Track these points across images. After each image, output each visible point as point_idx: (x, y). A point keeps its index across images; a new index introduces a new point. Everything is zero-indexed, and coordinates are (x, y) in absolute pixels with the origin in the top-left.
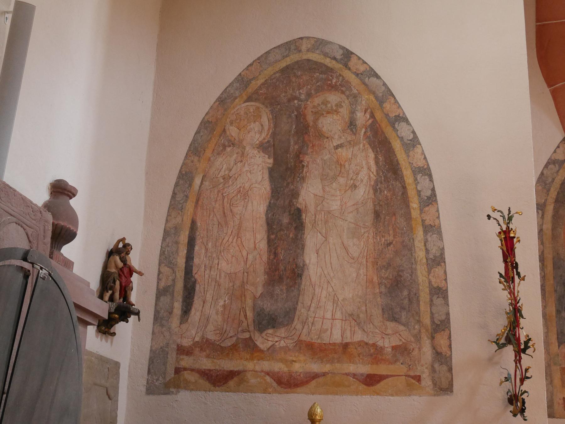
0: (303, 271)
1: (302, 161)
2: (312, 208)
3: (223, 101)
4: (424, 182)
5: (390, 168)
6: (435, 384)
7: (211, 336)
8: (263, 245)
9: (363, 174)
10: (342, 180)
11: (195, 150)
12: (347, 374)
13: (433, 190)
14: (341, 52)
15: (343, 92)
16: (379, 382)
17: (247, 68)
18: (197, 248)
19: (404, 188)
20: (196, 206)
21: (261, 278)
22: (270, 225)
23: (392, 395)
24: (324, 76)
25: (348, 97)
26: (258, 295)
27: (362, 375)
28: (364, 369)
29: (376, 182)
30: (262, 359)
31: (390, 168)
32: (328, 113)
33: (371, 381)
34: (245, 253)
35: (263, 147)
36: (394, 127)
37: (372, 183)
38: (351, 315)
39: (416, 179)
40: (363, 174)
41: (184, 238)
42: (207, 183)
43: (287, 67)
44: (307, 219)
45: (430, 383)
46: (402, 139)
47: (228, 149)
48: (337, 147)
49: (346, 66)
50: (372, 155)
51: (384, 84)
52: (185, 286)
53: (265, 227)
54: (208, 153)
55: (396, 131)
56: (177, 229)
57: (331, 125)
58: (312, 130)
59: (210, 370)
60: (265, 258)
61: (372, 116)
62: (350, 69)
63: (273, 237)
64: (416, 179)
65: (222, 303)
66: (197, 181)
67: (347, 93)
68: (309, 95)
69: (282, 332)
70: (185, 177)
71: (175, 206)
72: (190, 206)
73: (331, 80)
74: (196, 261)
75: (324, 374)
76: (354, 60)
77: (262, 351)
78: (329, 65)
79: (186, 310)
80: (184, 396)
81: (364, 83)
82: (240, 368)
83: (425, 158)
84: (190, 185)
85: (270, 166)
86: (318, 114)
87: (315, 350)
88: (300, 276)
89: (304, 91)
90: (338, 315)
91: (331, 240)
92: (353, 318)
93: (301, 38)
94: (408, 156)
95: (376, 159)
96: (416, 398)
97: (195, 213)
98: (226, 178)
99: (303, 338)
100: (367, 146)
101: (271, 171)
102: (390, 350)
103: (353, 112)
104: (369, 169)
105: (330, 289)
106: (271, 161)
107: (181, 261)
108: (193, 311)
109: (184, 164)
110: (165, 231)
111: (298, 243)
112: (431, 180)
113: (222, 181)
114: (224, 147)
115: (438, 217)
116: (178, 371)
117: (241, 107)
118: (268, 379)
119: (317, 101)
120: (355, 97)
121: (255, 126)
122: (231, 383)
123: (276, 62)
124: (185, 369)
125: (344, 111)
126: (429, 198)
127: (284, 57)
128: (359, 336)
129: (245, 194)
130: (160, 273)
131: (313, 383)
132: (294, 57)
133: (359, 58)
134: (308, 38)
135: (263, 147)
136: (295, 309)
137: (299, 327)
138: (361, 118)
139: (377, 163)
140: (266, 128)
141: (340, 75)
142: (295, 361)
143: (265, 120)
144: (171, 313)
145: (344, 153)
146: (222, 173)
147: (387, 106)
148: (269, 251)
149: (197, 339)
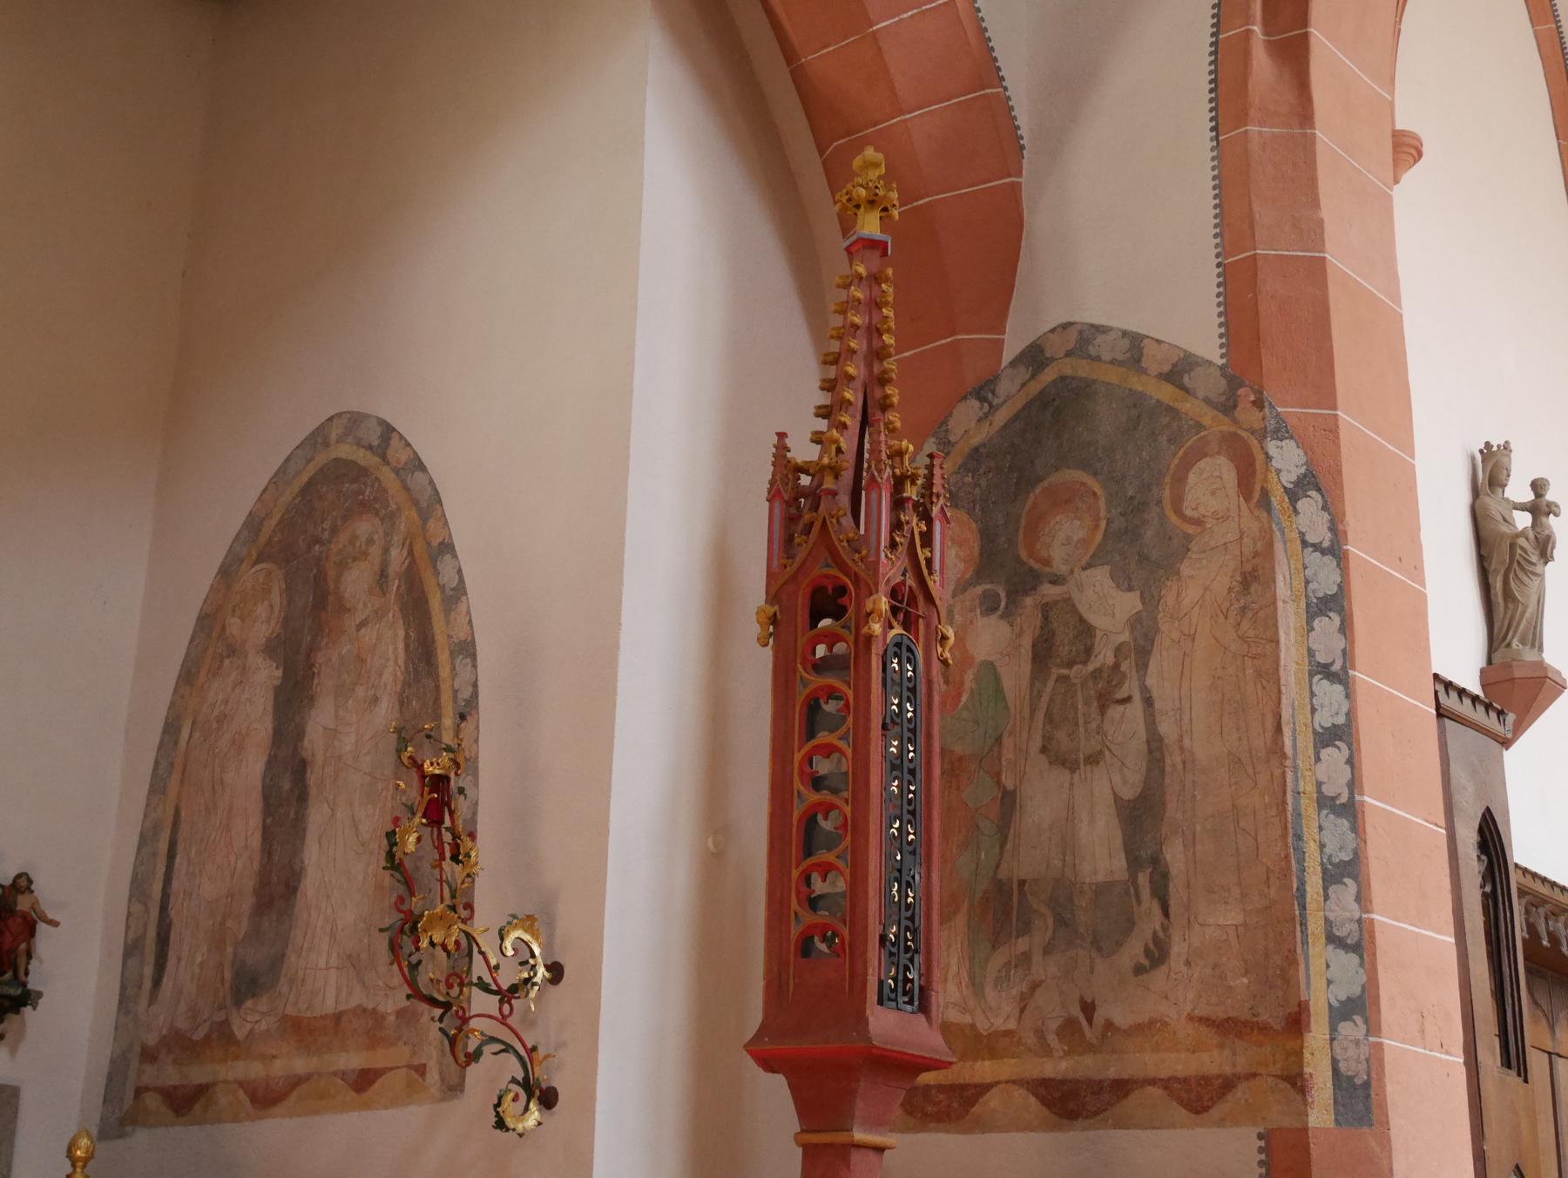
0: (299, 881)
1: (313, 665)
2: (319, 757)
3: (226, 573)
4: (465, 673)
5: (422, 653)
6: (443, 1080)
7: (182, 1024)
8: (256, 841)
9: (387, 676)
10: (360, 691)
11: (187, 676)
12: (335, 1074)
13: (475, 685)
14: (379, 430)
15: (377, 514)
16: (372, 1083)
17: (259, 499)
18: (178, 860)
19: (437, 688)
20: (182, 781)
21: (247, 904)
22: (267, 796)
23: (386, 1107)
24: (354, 486)
25: (382, 520)
26: (241, 936)
27: (353, 1071)
28: (353, 1060)
29: (404, 682)
30: (237, 1058)
31: (422, 653)
32: (354, 559)
33: (364, 1080)
34: (233, 859)
35: (270, 649)
36: (435, 567)
37: (399, 688)
38: (350, 957)
39: (453, 668)
40: (387, 676)
41: (163, 847)
42: (197, 734)
43: (311, 483)
44: (312, 778)
45: (437, 1077)
46: (442, 588)
47: (227, 662)
48: (359, 627)
49: (384, 457)
50: (401, 633)
51: (431, 481)
52: (158, 934)
53: (260, 805)
54: (202, 677)
55: (437, 573)
56: (157, 828)
57: (355, 582)
58: (331, 598)
59: (175, 1087)
60: (256, 866)
61: (411, 552)
62: (388, 464)
63: (269, 820)
64: (453, 668)
65: (199, 960)
66: (185, 734)
67: (383, 512)
68: (334, 530)
69: (263, 1003)
70: (171, 728)
71: (157, 788)
72: (173, 784)
73: (362, 493)
74: (175, 884)
75: (307, 1078)
76: (395, 441)
77: (237, 1043)
78: (362, 463)
79: (157, 982)
80: (141, 1138)
81: (406, 488)
82: (203, 1080)
83: (470, 621)
84: (176, 743)
85: (277, 682)
86: (342, 566)
87: (302, 1030)
88: (295, 890)
89: (327, 525)
90: (334, 961)
91: (339, 815)
92: (354, 963)
93: (331, 419)
94: (448, 622)
95: (407, 636)
96: (413, 1109)
97: (179, 795)
98: (221, 719)
99: (290, 1011)
100: (399, 615)
101: (278, 691)
102: (392, 1018)
103: (386, 551)
104: (396, 661)
105: (329, 911)
106: (279, 673)
107: (157, 888)
108: (165, 980)
109: (172, 704)
110: (142, 836)
111: (298, 828)
112: (475, 666)
113: (215, 726)
114: (222, 659)
115: (476, 741)
116: (139, 1092)
117: (250, 576)
118: (241, 1094)
119: (343, 538)
120: (392, 517)
121: (261, 610)
122: (197, 1107)
123: (298, 474)
124: (147, 1089)
125: (375, 551)
126: (468, 702)
127: (309, 461)
128: (357, 998)
129: (238, 745)
130: (129, 914)
131: (293, 1097)
132: (321, 459)
133: (402, 437)
134: (339, 415)
135: (270, 649)
136: (283, 955)
137: (285, 989)
138: (397, 556)
139: (407, 646)
140: (277, 608)
141: (377, 479)
142: (275, 1057)
143: (276, 597)
144: (140, 988)
145: (368, 635)
146: (216, 713)
147: (431, 524)
148: (263, 850)
149: (164, 1032)
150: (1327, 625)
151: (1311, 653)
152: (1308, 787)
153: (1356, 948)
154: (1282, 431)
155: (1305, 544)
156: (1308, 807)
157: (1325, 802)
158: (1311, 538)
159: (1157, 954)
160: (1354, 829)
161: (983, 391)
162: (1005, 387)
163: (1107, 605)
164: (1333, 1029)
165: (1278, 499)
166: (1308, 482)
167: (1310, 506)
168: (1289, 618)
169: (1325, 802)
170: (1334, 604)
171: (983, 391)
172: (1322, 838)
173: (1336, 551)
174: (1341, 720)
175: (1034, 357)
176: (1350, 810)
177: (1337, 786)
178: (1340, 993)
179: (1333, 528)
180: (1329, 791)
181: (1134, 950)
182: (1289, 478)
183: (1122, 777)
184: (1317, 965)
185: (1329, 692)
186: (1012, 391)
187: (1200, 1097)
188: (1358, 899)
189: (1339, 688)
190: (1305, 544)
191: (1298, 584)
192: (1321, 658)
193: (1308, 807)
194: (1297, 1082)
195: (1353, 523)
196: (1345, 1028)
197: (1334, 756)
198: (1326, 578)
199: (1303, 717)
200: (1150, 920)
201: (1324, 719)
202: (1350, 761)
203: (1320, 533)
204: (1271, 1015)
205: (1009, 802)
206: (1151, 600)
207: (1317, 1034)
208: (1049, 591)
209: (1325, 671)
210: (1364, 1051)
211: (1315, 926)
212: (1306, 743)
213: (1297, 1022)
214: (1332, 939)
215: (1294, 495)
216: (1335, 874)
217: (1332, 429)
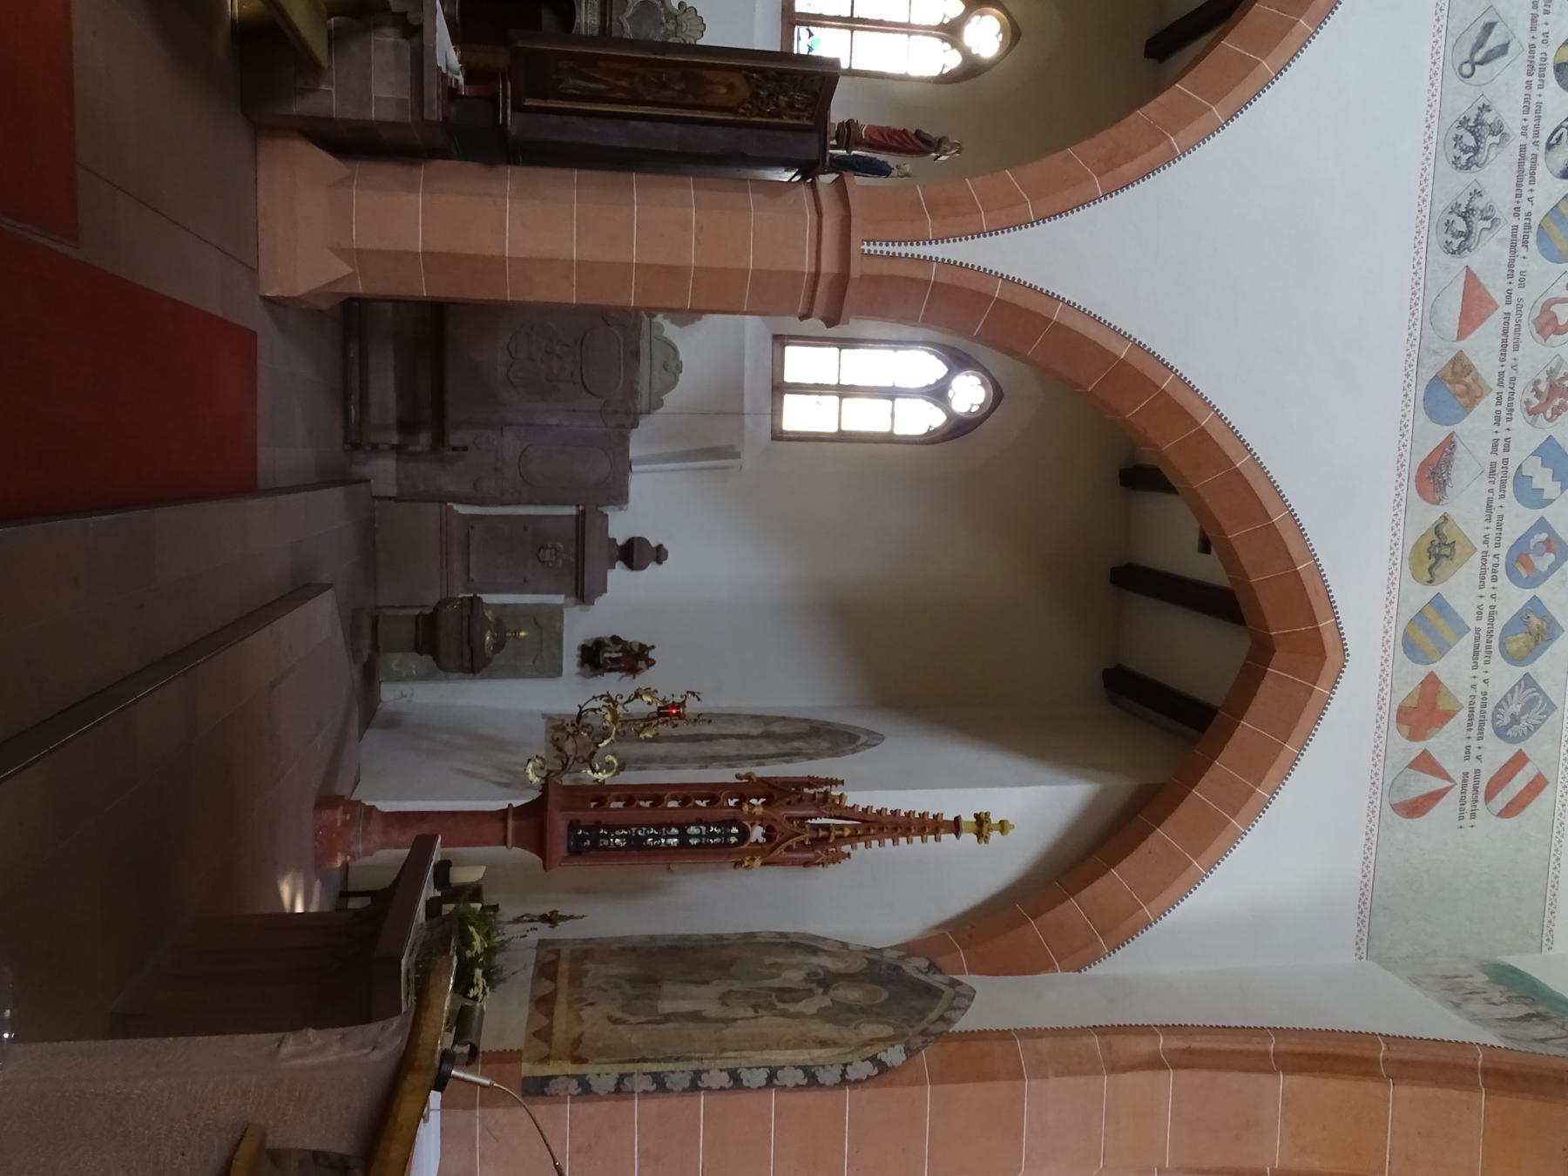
150: (800, 1077)
151: (782, 1068)
152: (706, 1065)
153: (618, 1090)
154: (910, 1052)
155: (845, 1065)
156: (694, 1065)
157: (697, 1074)
158: (849, 1068)
159: (616, 1021)
160: (684, 1090)
161: (933, 967)
162: (938, 977)
163: (808, 1006)
164: (573, 1076)
165: (870, 1051)
166: (883, 1068)
167: (867, 1069)
168: (803, 1056)
169: (697, 1074)
170: (812, 1081)
171: (933, 967)
172: (678, 1075)
173: (844, 1082)
174: (745, 1083)
175: (954, 984)
176: (694, 1087)
177: (706, 1081)
178: (593, 1081)
179: (857, 1082)
180: (704, 1076)
181: (618, 1014)
182: (882, 1056)
183: (711, 1008)
184: (607, 1068)
185: (760, 1077)
186: (936, 980)
187: (543, 1035)
188: (645, 1092)
189: (764, 1083)
190: (845, 1065)
191: (821, 1062)
192: (779, 1073)
193: (694, 1065)
194: (545, 1059)
195: (865, 1094)
196: (574, 1083)
197: (724, 1079)
198: (829, 1077)
199: (744, 1063)
200: (633, 1019)
201: (745, 1074)
202: (722, 1089)
203: (852, 1074)
204: (581, 1052)
205: (706, 982)
206: (812, 1016)
207: (571, 1069)
208: (820, 991)
209: (772, 1076)
210: (562, 1093)
211: (629, 1068)
212: (731, 1064)
213: (578, 1060)
214: (622, 1077)
215: (873, 1059)
216: (657, 1078)
217: (918, 1081)
